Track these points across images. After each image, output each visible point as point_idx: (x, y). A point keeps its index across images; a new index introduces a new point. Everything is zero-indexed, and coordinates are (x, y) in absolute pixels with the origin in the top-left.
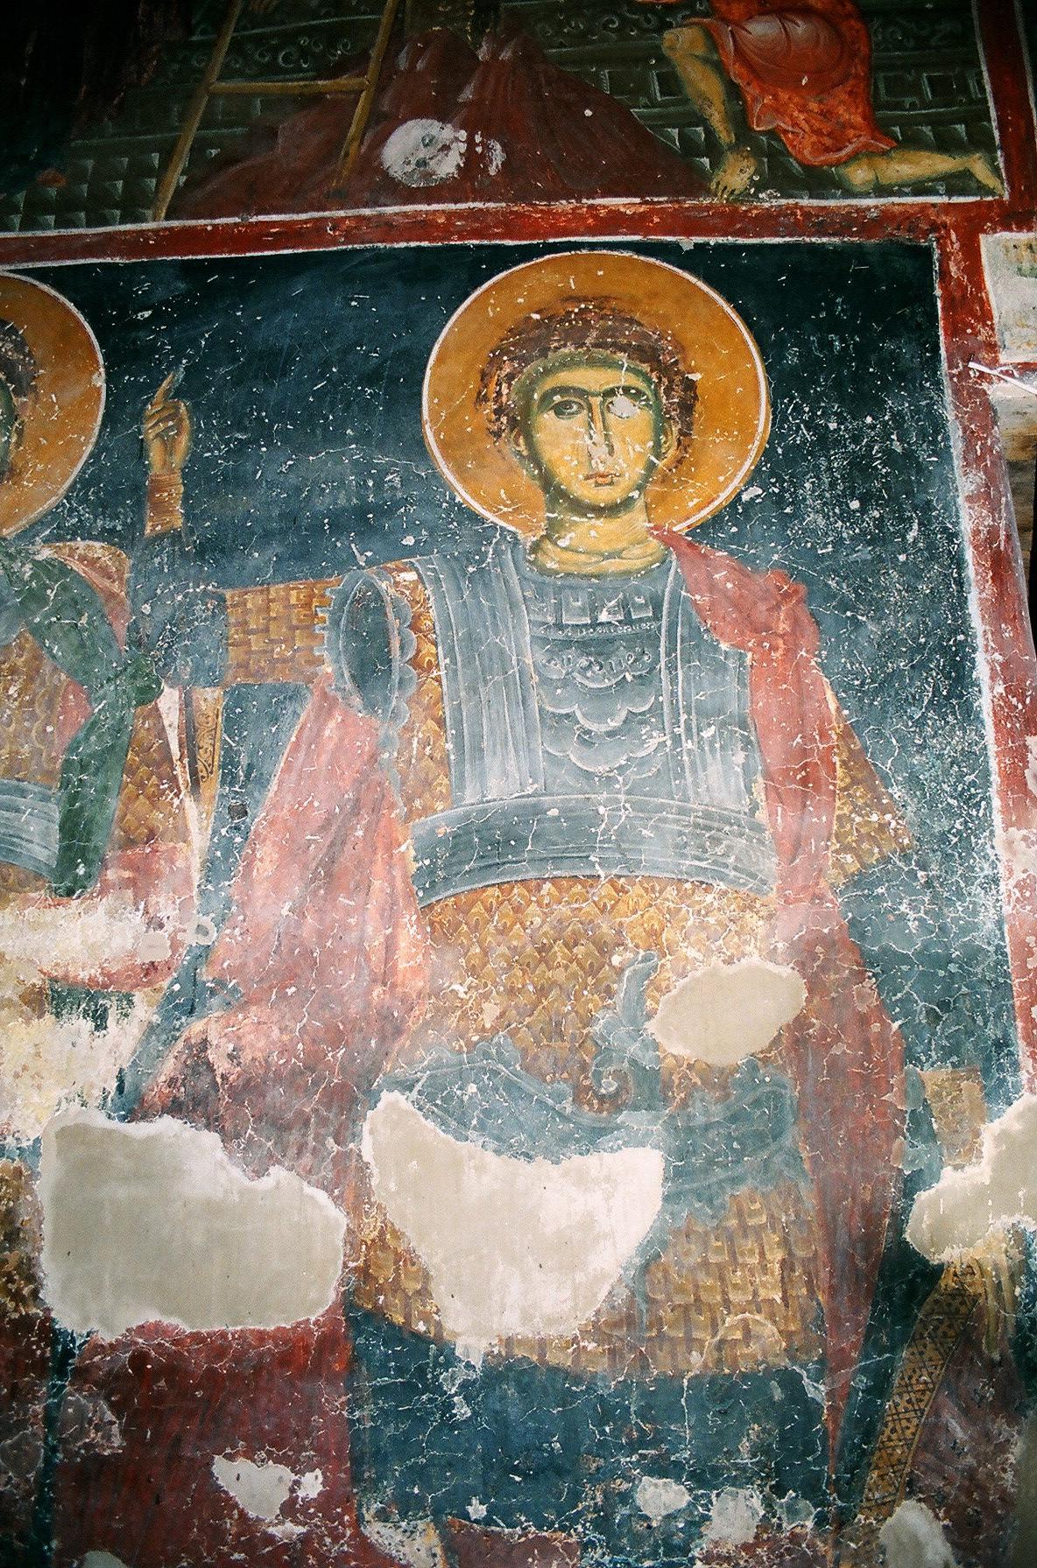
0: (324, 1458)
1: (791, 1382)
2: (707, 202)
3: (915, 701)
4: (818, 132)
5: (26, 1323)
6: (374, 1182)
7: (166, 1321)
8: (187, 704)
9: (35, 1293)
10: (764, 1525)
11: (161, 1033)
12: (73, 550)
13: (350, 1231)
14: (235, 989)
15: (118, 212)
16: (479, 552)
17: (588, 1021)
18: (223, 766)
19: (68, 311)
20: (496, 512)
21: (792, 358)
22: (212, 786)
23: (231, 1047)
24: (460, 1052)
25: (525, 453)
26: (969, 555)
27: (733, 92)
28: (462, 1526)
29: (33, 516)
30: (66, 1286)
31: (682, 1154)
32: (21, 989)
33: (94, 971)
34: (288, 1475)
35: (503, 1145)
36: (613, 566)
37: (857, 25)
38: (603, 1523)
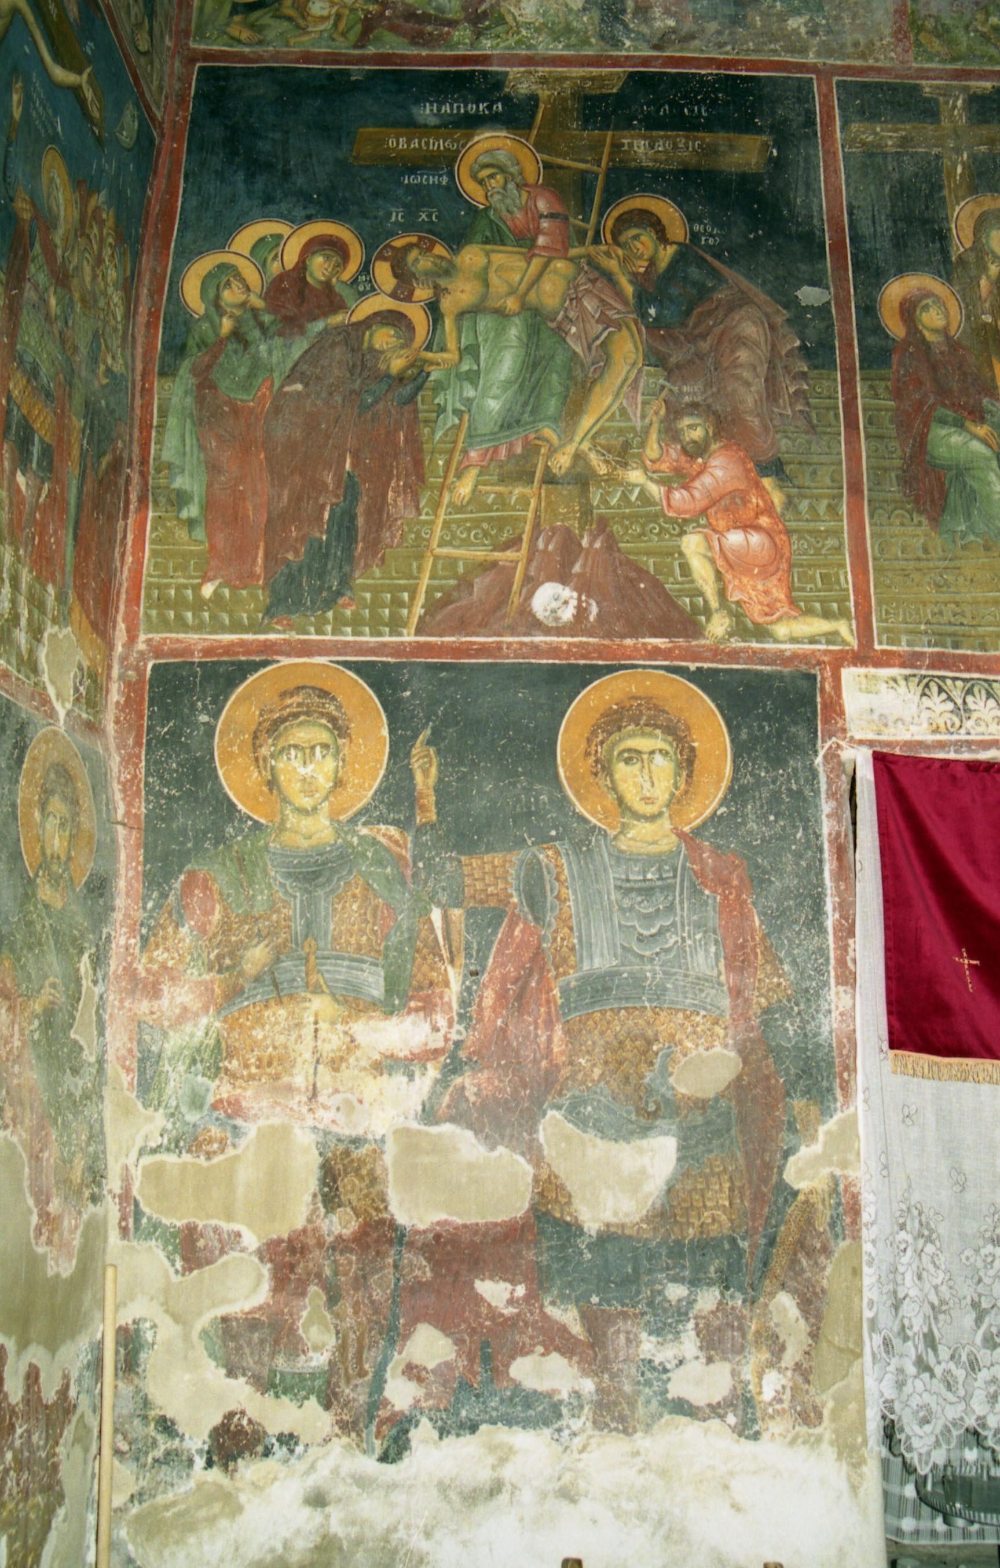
0: (527, 1280)
1: (733, 1241)
2: (703, 642)
3: (796, 922)
4: (761, 603)
5: (382, 1222)
6: (546, 1152)
8: (446, 918)
10: (720, 1303)
11: (442, 1082)
17: (642, 1077)
21: (744, 736)
22: (461, 960)
26: (826, 846)
27: (719, 576)
29: (355, 809)
30: (401, 1203)
31: (685, 1139)
33: (407, 1053)
35: (604, 1135)
36: (653, 849)
37: (784, 537)
38: (650, 1304)
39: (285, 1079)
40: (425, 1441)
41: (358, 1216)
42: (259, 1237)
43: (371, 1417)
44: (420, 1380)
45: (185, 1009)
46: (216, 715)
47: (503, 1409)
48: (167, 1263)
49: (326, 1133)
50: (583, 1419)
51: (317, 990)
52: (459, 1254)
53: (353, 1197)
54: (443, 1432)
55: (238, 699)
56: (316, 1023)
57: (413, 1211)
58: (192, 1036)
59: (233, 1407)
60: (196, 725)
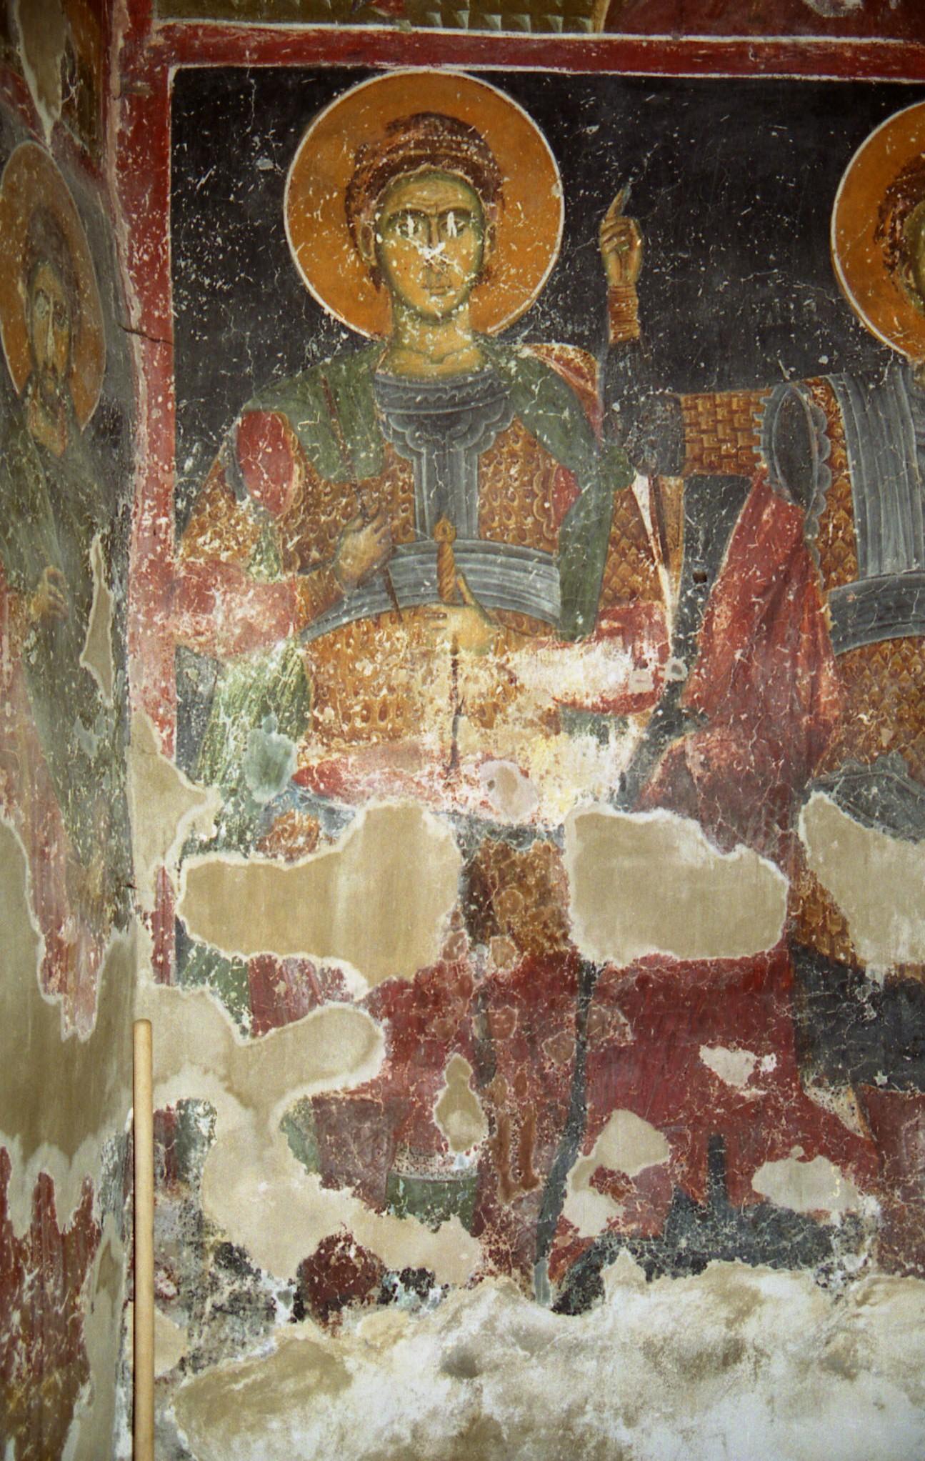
0: (778, 1046)
5: (559, 957)
6: (808, 855)
7: (662, 954)
8: (656, 491)
9: (565, 936)
11: (651, 746)
12: (550, 351)
13: (791, 890)
14: (702, 714)
15: (560, 19)
16: (877, 372)
18: (687, 541)
19: (525, 120)
20: (890, 337)
22: (680, 557)
23: (702, 757)
24: (866, 763)
25: (913, 285)
28: (871, 1090)
30: (587, 931)
32: (539, 712)
33: (597, 700)
34: (752, 1057)
39: (409, 738)
40: (626, 1283)
41: (522, 948)
42: (370, 978)
43: (543, 1248)
44: (617, 1193)
45: (249, 628)
46: (285, 159)
47: (743, 1238)
48: (230, 1020)
49: (473, 821)
50: (864, 1256)
51: (456, 601)
52: (676, 1006)
53: (515, 920)
54: (652, 1271)
55: (313, 139)
56: (455, 652)
57: (605, 941)
58: (262, 668)
59: (334, 1231)
60: (254, 175)
